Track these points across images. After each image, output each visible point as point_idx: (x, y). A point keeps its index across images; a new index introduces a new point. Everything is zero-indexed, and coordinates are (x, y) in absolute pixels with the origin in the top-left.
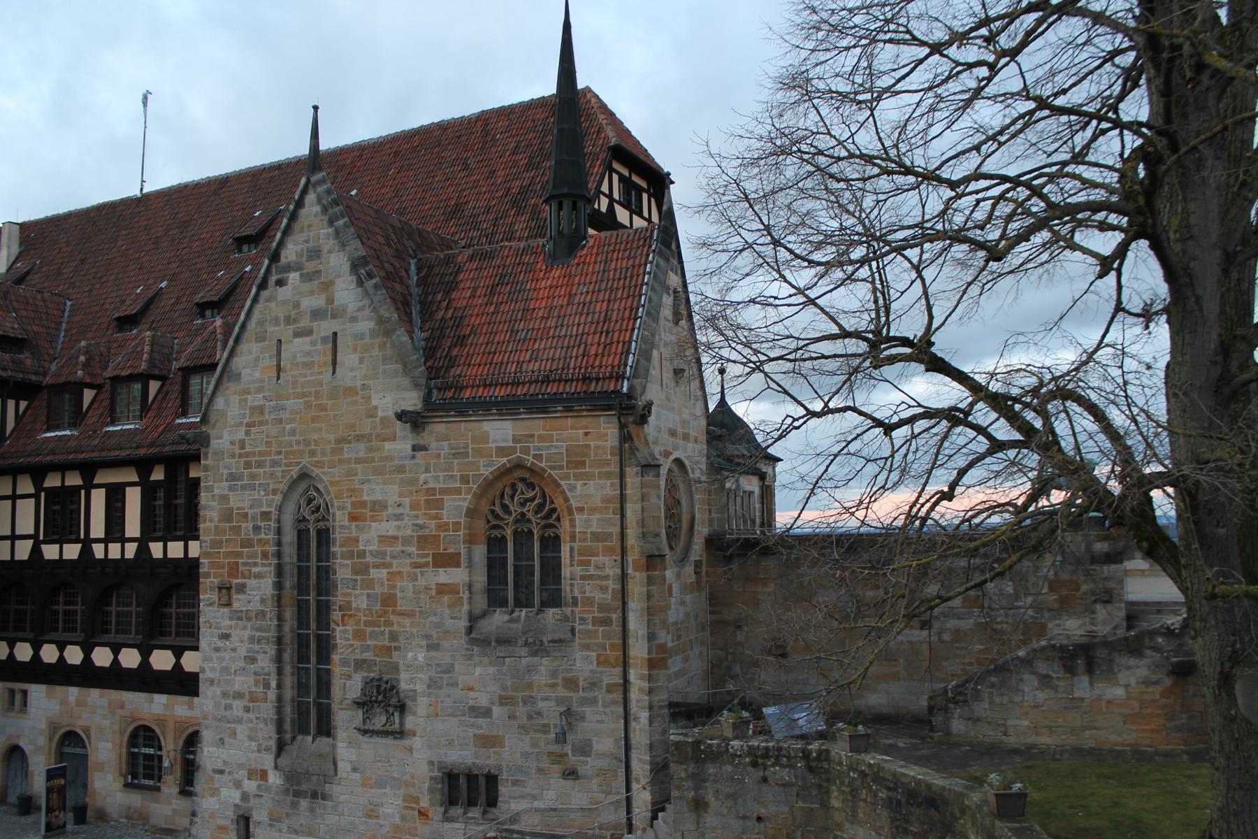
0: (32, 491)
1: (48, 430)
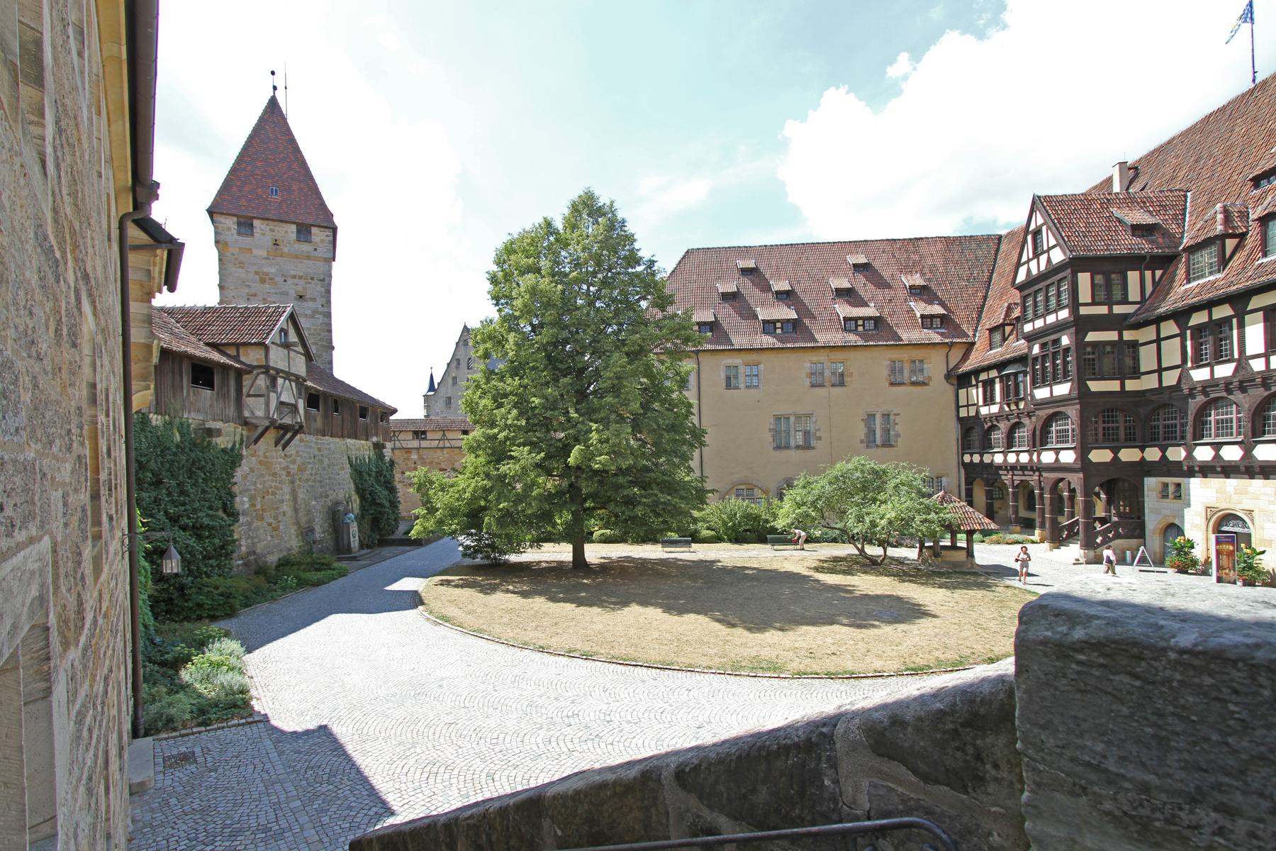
0: (1178, 331)
1: (1189, 282)
